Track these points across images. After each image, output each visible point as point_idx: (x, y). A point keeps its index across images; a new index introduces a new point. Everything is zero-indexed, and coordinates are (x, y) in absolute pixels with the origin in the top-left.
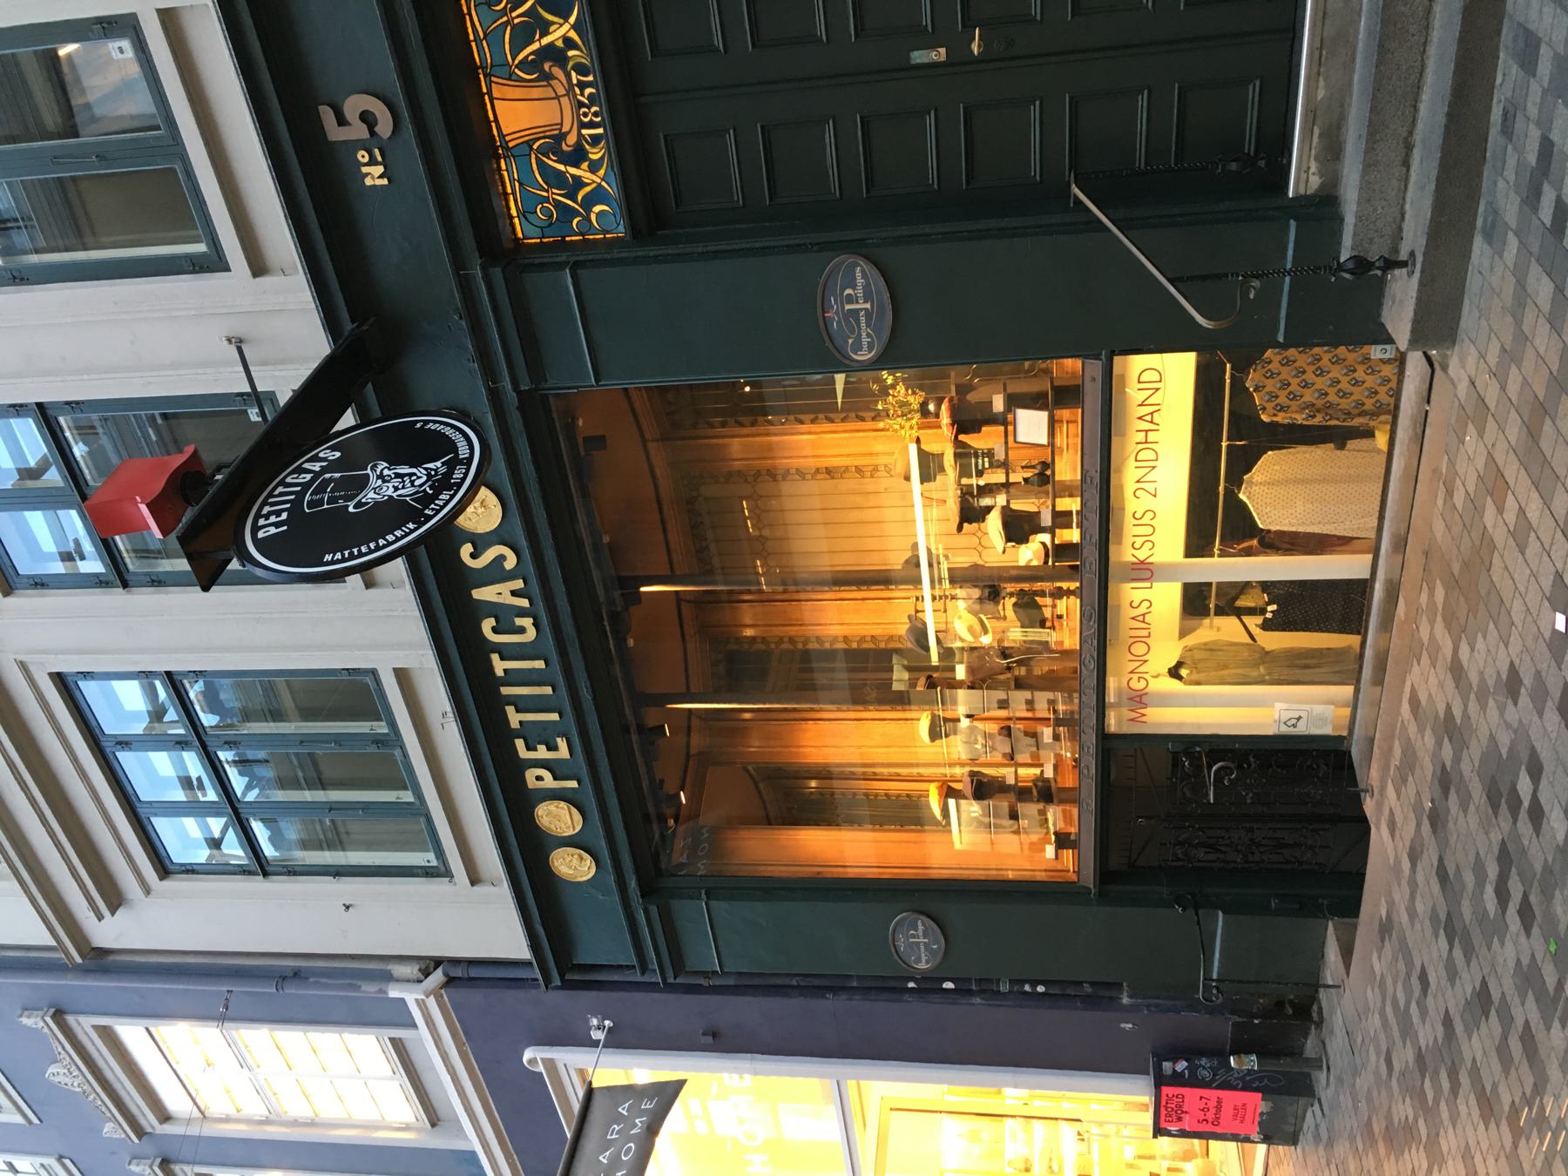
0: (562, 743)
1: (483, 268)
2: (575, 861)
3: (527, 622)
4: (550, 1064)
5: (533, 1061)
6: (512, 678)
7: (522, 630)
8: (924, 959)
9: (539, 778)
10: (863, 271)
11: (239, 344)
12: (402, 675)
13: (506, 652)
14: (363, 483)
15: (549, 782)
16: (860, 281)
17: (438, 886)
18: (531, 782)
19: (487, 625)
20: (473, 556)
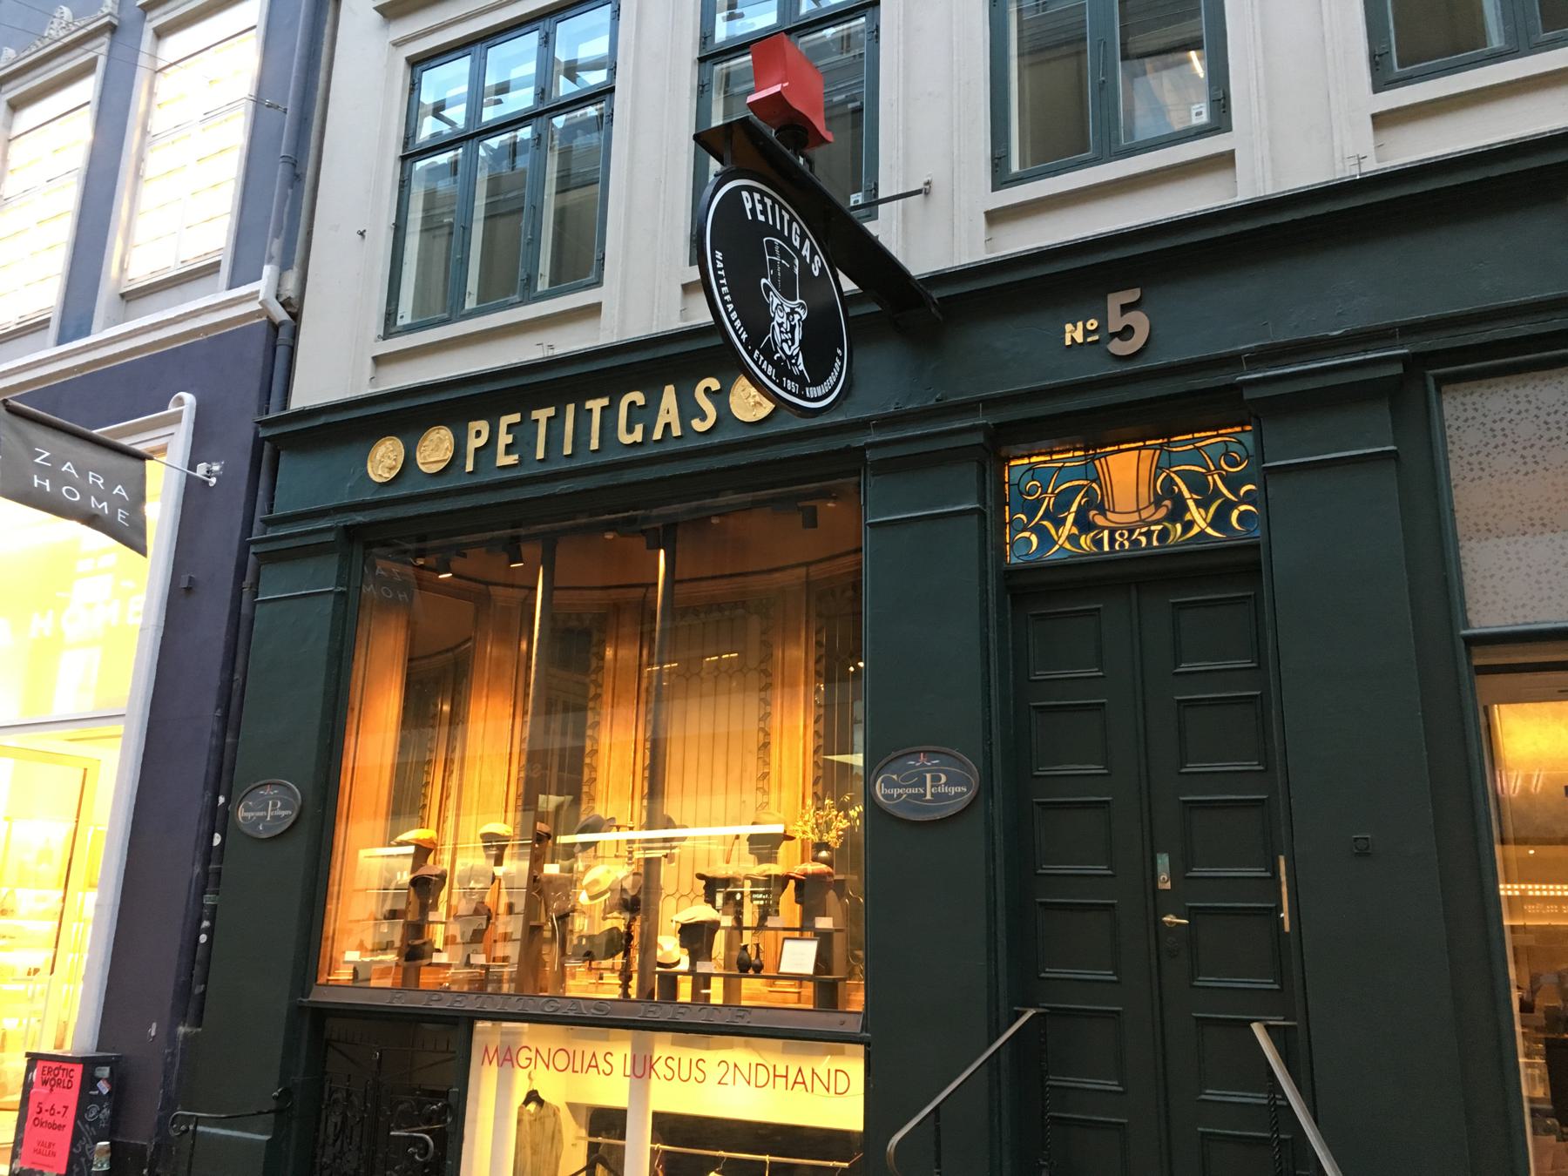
0: (512, 459)
3: (638, 436)
4: (176, 419)
5: (180, 402)
6: (583, 417)
7: (630, 430)
8: (249, 815)
9: (478, 434)
10: (962, 794)
11: (925, 191)
12: (594, 310)
13: (609, 413)
15: (474, 443)
16: (953, 790)
17: (376, 324)
18: (474, 426)
19: (638, 397)
20: (707, 390)
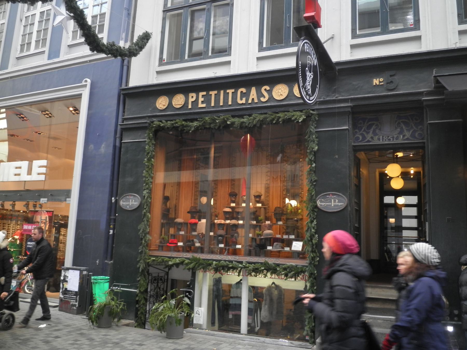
0: (204, 105)
1: (350, 106)
2: (163, 104)
3: (244, 101)
4: (85, 86)
5: (86, 81)
6: (226, 95)
7: (241, 99)
8: (124, 203)
9: (192, 97)
10: (342, 205)
11: (332, 38)
12: (229, 63)
13: (234, 94)
14: (310, 72)
15: (191, 100)
16: (340, 204)
17: (157, 63)
18: (191, 95)
19: (244, 90)
20: (265, 89)
